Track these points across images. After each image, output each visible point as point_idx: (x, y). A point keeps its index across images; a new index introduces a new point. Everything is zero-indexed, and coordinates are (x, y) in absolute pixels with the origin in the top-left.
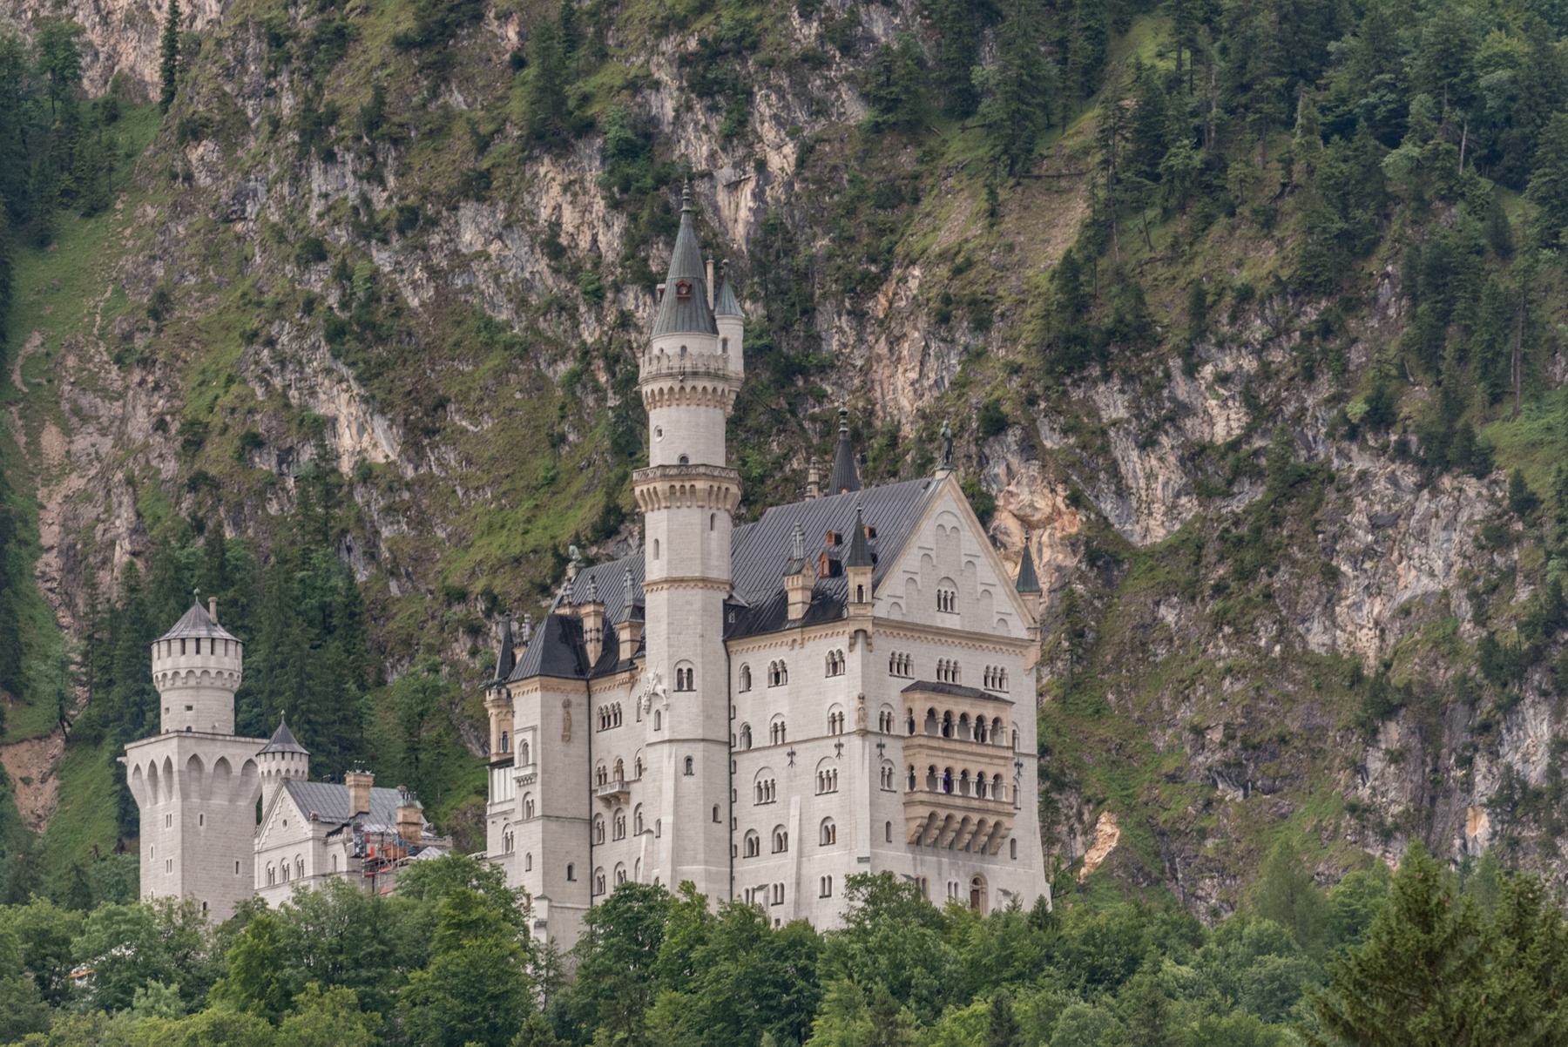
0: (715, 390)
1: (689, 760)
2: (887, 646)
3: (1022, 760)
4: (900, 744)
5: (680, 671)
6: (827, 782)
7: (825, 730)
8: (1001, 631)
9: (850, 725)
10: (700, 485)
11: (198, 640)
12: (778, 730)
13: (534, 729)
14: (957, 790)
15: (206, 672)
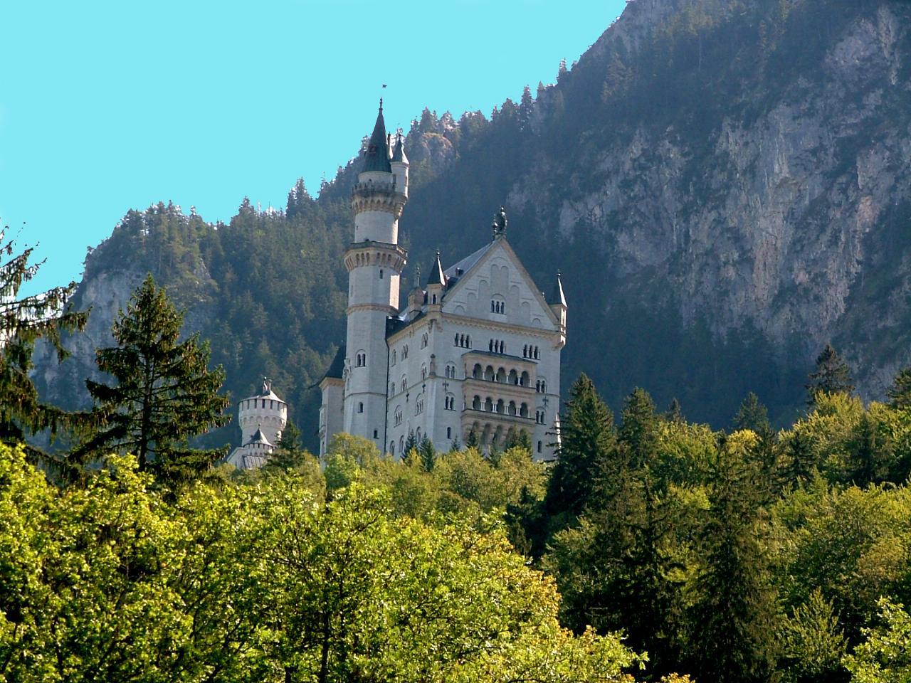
0: (385, 202)
1: (362, 405)
2: (452, 330)
3: (547, 398)
4: (461, 384)
5: (359, 356)
6: (420, 407)
7: (419, 378)
8: (536, 325)
9: (427, 375)
10: (372, 252)
11: (256, 400)
12: (404, 384)
13: (325, 406)
14: (494, 410)
15: (259, 417)
